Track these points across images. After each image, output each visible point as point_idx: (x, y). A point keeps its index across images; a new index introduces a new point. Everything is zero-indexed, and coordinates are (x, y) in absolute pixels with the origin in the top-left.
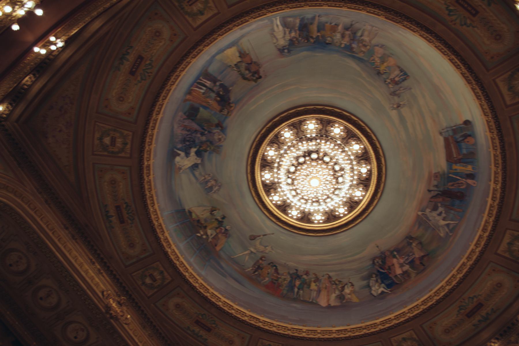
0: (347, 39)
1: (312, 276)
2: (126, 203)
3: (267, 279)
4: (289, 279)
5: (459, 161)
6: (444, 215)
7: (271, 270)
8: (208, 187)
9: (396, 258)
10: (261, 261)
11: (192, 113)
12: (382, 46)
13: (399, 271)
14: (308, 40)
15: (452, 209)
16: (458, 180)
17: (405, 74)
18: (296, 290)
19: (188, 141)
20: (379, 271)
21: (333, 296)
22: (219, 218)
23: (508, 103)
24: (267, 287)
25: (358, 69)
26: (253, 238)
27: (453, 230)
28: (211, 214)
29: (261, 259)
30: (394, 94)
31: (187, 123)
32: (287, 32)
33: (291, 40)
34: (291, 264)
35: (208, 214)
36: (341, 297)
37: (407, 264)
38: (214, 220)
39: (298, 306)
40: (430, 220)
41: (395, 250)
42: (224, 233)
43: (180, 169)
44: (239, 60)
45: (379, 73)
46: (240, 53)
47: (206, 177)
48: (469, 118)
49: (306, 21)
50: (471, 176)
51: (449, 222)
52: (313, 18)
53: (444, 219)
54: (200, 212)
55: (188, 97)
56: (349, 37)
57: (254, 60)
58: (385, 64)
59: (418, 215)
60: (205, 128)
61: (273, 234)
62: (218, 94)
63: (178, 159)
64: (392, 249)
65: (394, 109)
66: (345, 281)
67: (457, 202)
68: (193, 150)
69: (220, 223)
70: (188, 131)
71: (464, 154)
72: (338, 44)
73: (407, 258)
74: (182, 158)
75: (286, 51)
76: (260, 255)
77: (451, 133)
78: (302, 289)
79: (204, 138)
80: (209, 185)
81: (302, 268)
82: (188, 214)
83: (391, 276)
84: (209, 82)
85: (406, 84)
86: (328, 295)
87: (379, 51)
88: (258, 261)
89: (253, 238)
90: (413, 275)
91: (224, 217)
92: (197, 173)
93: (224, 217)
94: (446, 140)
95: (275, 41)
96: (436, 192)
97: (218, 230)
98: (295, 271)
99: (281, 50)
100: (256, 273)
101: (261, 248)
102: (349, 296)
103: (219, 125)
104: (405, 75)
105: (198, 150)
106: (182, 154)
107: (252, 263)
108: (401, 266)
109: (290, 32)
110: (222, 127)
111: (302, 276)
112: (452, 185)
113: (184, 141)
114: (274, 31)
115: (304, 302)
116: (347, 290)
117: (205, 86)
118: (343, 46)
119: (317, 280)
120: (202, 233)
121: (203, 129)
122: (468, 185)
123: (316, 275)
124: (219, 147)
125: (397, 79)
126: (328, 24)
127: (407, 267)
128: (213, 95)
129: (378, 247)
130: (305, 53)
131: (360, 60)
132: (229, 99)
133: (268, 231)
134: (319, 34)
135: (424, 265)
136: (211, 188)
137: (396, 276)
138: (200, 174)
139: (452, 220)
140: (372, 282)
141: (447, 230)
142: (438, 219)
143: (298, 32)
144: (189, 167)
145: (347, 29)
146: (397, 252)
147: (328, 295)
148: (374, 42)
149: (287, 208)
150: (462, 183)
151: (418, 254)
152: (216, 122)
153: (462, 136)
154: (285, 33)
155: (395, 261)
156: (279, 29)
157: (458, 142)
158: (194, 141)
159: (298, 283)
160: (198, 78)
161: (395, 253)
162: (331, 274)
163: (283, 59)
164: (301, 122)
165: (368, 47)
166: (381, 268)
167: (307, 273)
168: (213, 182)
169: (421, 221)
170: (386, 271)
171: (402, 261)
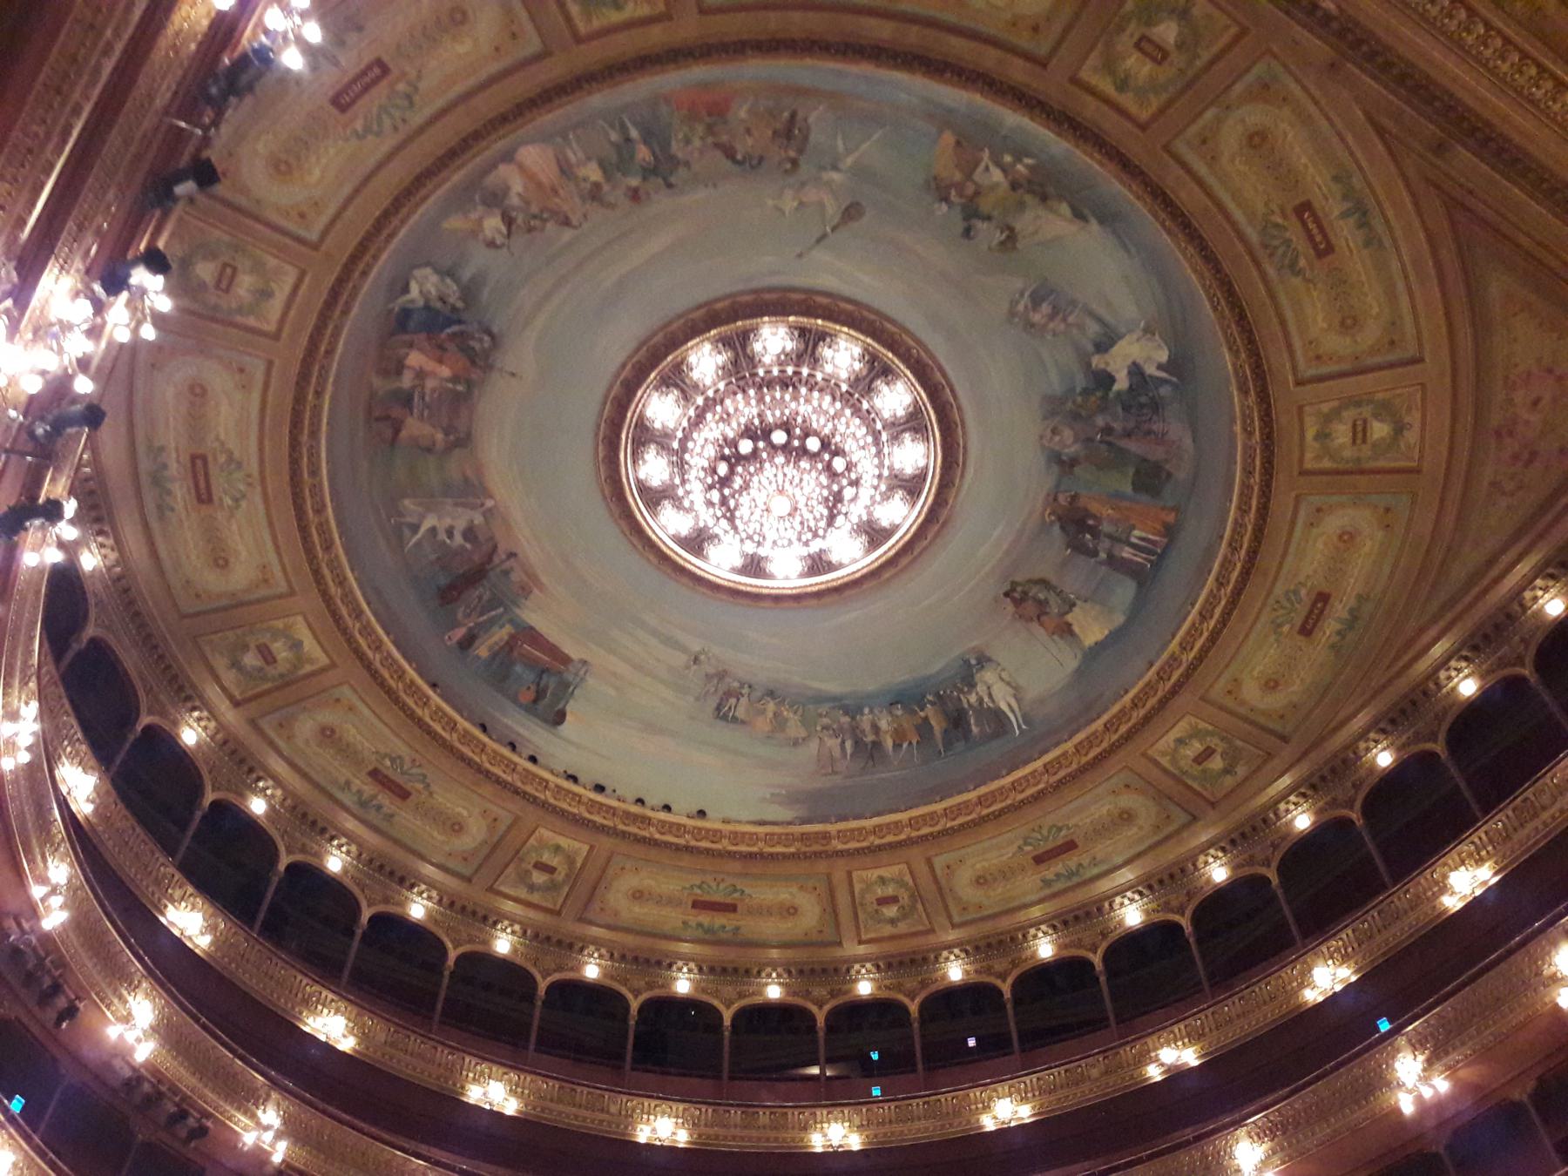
0: (866, 726)
1: (616, 195)
3: (743, 114)
4: (676, 148)
5: (510, 644)
6: (442, 536)
8: (1048, 298)
9: (448, 380)
10: (792, 154)
13: (415, 359)
14: (937, 695)
15: (438, 559)
16: (482, 614)
17: (724, 718)
18: (634, 133)
19: (1142, 406)
20: (460, 322)
21: (517, 185)
22: (981, 226)
25: (816, 685)
26: (851, 212)
28: (1011, 229)
29: (795, 163)
30: (722, 675)
31: (1158, 454)
32: (986, 699)
33: (972, 686)
34: (701, 194)
35: (1018, 226)
36: (495, 199)
37: (413, 388)
38: (995, 213)
40: (456, 505)
42: (948, 187)
43: (1148, 331)
44: (1069, 618)
45: (771, 694)
47: (1062, 326)
48: (561, 728)
50: (468, 642)
51: (419, 536)
53: (433, 530)
54: (1050, 225)
55: (1171, 518)
56: (863, 731)
57: (1035, 626)
58: (770, 715)
59: (491, 497)
60: (1103, 447)
61: (800, 256)
63: (1163, 356)
64: (476, 392)
66: (519, 240)
67: (443, 581)
69: (971, 213)
70: (1149, 432)
73: (427, 398)
74: (1149, 359)
75: (973, 662)
76: (805, 169)
78: (617, 146)
81: (662, 202)
82: (1086, 212)
83: (423, 336)
84: (1125, 555)
85: (713, 703)
87: (795, 729)
88: (801, 151)
89: (851, 212)
90: (377, 382)
91: (967, 233)
92: (1093, 328)
93: (967, 233)
94: (566, 660)
95: (1004, 675)
96: (496, 560)
97: (970, 189)
98: (673, 180)
99: (983, 660)
100: (786, 114)
101: (811, 194)
102: (474, 216)
104: (722, 714)
105: (1109, 388)
106: (1151, 370)
107: (816, 137)
108: (421, 374)
109: (981, 700)
110: (1061, 462)
111: (645, 179)
112: (480, 598)
113: (1156, 406)
114: (1015, 696)
116: (493, 224)
117: (1134, 546)
118: (866, 710)
120: (1019, 167)
121: (1109, 444)
122: (455, 624)
124: (1052, 414)
125: (733, 701)
127: (407, 381)
128: (1106, 527)
129: (513, 375)
131: (820, 698)
132: (1062, 528)
133: (820, 255)
135: (377, 419)
136: (1036, 301)
137: (411, 345)
138: (1081, 327)
139: (418, 544)
140: (452, 290)
141: (409, 519)
142: (445, 522)
144: (1121, 337)
145: (874, 743)
146: (457, 394)
148: (814, 745)
150: (469, 615)
151: (415, 427)
153: (547, 687)
154: (990, 696)
155: (445, 372)
156: (1004, 700)
157: (543, 672)
158: (1126, 409)
159: (643, 153)
161: (460, 388)
162: (568, 234)
163: (973, 644)
166: (462, 333)
167: (635, 195)
168: (1036, 318)
169: (471, 490)
170: (443, 335)
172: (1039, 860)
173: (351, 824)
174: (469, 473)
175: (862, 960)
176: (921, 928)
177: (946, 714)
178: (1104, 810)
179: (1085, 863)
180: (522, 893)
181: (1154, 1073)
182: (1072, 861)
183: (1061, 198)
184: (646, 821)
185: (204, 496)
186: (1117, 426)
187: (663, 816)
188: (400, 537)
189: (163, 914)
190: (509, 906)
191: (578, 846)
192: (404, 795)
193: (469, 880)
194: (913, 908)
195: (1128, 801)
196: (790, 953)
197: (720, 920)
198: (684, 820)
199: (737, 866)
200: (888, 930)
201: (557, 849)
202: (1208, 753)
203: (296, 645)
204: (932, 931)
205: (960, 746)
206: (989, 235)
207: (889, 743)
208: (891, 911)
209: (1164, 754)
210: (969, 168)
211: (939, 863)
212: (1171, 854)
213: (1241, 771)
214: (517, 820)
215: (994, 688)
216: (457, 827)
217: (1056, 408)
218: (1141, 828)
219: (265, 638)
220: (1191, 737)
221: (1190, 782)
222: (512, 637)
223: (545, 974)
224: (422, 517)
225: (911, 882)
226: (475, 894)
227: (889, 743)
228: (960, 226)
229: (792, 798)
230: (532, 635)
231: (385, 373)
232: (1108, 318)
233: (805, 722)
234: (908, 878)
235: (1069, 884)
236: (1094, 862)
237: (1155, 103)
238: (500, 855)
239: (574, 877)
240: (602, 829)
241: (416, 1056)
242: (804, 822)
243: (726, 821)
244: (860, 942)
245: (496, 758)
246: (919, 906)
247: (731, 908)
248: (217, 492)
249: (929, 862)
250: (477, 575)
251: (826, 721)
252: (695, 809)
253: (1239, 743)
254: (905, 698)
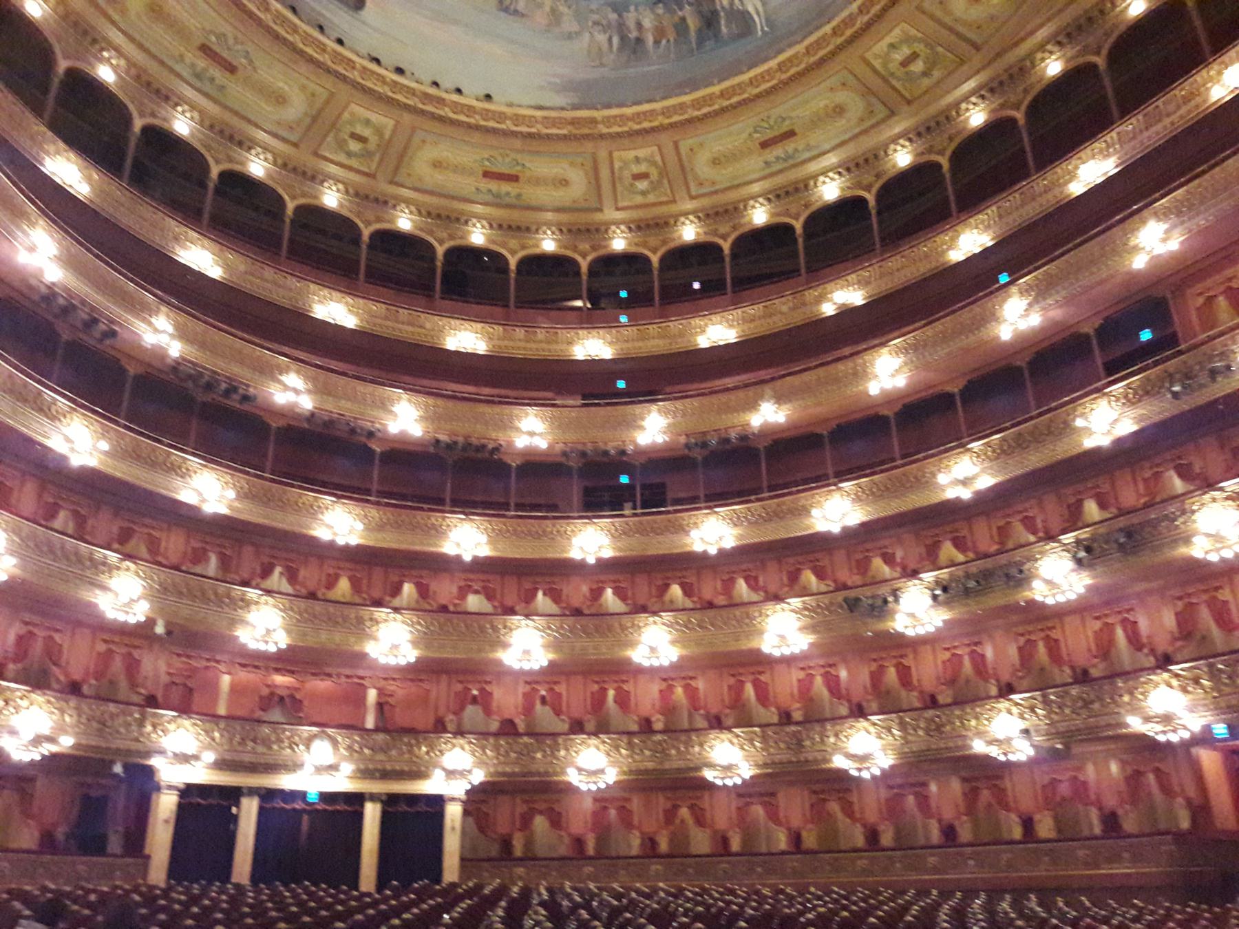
0: (631, 23)
12: (569, 36)
17: (506, 10)
23: (353, 105)
58: (547, 9)
72: (641, 9)
87: (569, 24)
118: (632, 8)
126: (672, 39)
134: (680, 13)
143: (719, 8)
148: (587, 36)
165: (590, 24)
172: (765, 145)
173: (189, 93)
175: (617, 223)
176: (664, 199)
178: (822, 104)
179: (800, 148)
180: (342, 158)
181: (828, 309)
182: (790, 146)
184: (441, 101)
187: (455, 97)
189: (43, 165)
190: (333, 169)
191: (383, 120)
192: (231, 69)
193: (295, 145)
194: (660, 182)
195: (842, 97)
196: (564, 218)
197: (505, 187)
198: (475, 103)
199: (518, 143)
200: (639, 199)
201: (367, 122)
202: (914, 56)
204: (674, 201)
205: (709, 44)
207: (650, 40)
208: (642, 185)
209: (876, 56)
211: (684, 146)
212: (868, 142)
213: (937, 74)
214: (332, 94)
216: (280, 100)
218: (848, 121)
220: (901, 42)
221: (894, 82)
223: (368, 223)
225: (660, 163)
226: (303, 157)
227: (650, 40)
229: (568, 86)
234: (658, 158)
235: (786, 165)
236: (808, 148)
238: (320, 125)
239: (385, 147)
240: (407, 107)
241: (274, 283)
242: (575, 107)
243: (510, 105)
244: (618, 209)
245: (307, 38)
246: (665, 181)
247: (513, 178)
249: (676, 145)
251: (596, 17)
252: (482, 93)
253: (940, 49)
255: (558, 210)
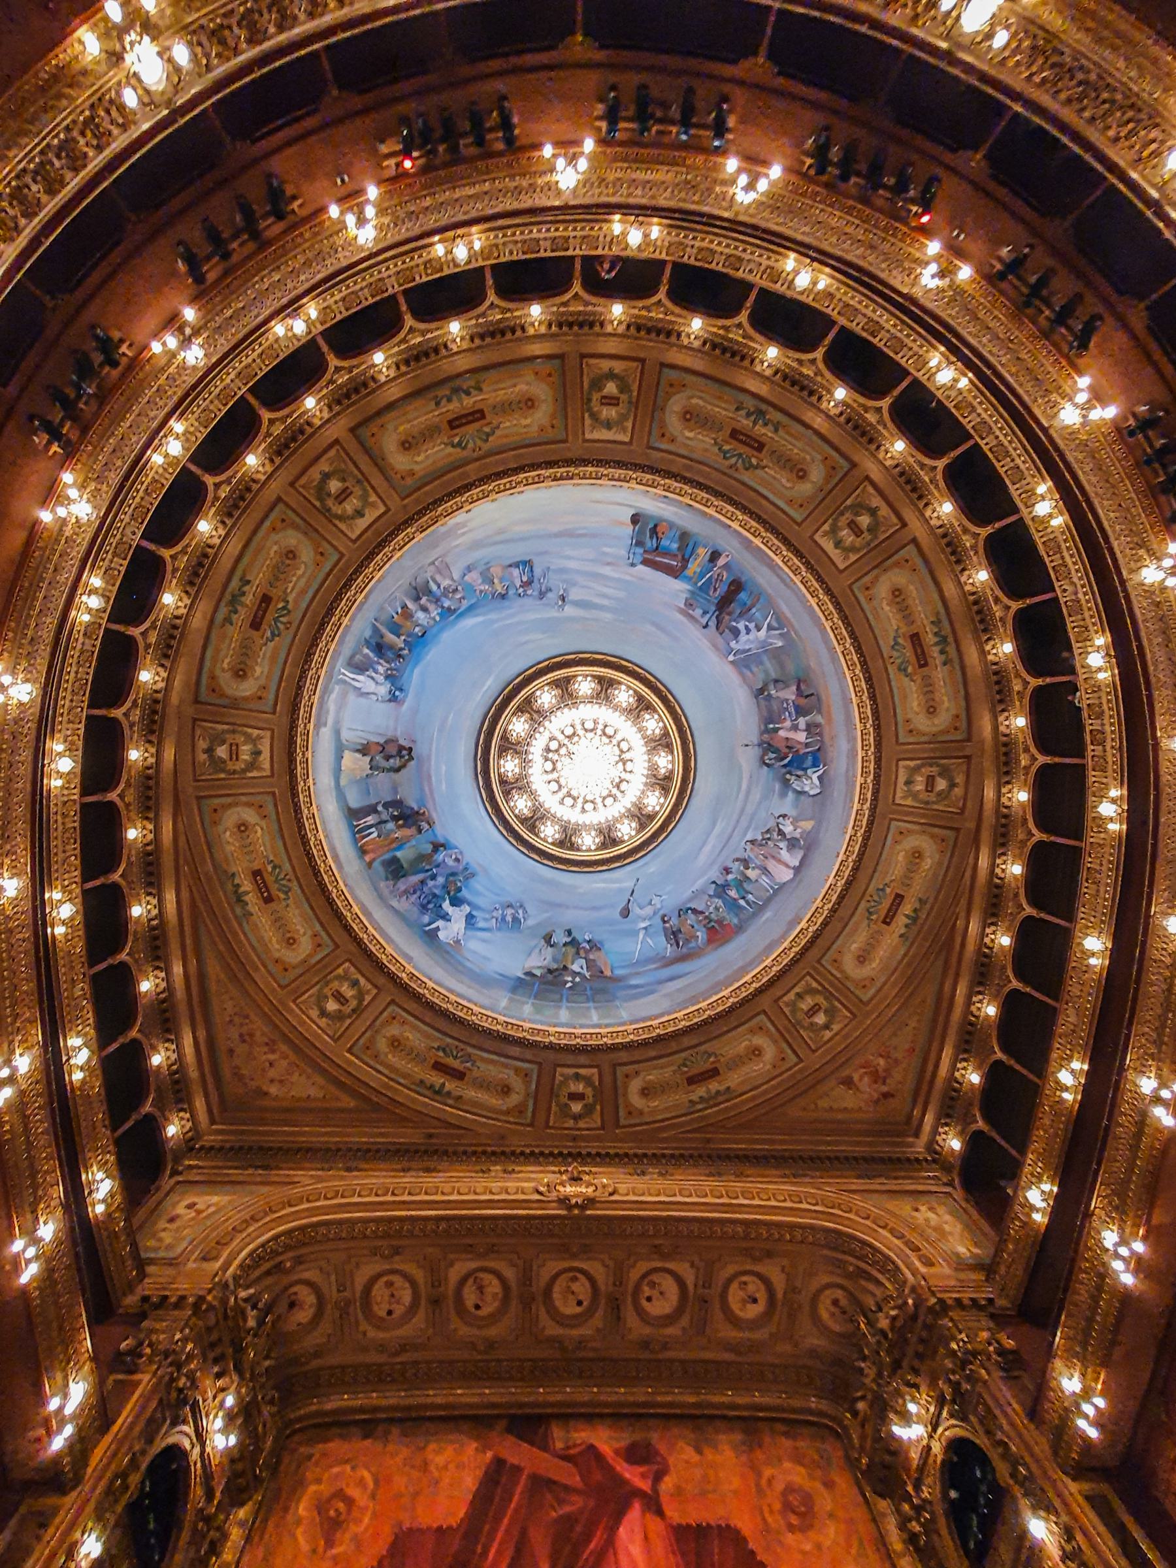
0: (431, 607)
1: (736, 867)
2: (438, 1049)
4: (720, 903)
5: (685, 561)
6: (752, 626)
7: (691, 919)
8: (511, 920)
11: (395, 870)
12: (469, 569)
13: (801, 737)
14: (400, 656)
17: (525, 563)
18: (742, 902)
20: (785, 766)
21: (785, 854)
24: (710, 941)
25: (480, 619)
26: (625, 913)
27: (781, 622)
30: (542, 595)
31: (402, 885)
33: (387, 677)
36: (793, 844)
39: (768, 914)
41: (767, 723)
44: (368, 759)
45: (503, 597)
46: (358, 751)
48: (632, 512)
49: (373, 642)
50: (715, 556)
52: (375, 630)
54: (540, 960)
55: (367, 858)
57: (382, 741)
62: (395, 818)
63: (441, 935)
65: (562, 607)
67: (743, 596)
68: (446, 905)
69: (574, 943)
71: (679, 549)
76: (657, 920)
77: (640, 550)
79: (441, 880)
80: (509, 918)
81: (714, 874)
85: (538, 571)
86: (780, 861)
87: (474, 577)
88: (665, 929)
90: (819, 719)
91: (569, 932)
93: (569, 932)
94: (645, 562)
97: (582, 953)
99: (393, 699)
101: (649, 910)
103: (437, 847)
108: (795, 728)
110: (443, 845)
113: (424, 908)
115: (768, 900)
116: (788, 829)
119: (746, 863)
122: (726, 566)
123: (737, 860)
125: (525, 579)
127: (802, 722)
128: (391, 825)
130: (417, 671)
133: (629, 884)
136: (515, 919)
137: (807, 745)
138: (486, 920)
140: (796, 785)
145: (417, 599)
147: (780, 861)
148: (456, 576)
149: (613, 835)
151: (790, 694)
152: (429, 848)
155: (782, 733)
156: (363, 681)
158: (435, 895)
159: (733, 893)
160: (352, 827)
162: (749, 837)
164: (505, 737)
168: (510, 911)
169: (744, 662)
171: (788, 724)
174: (748, 673)
177: (391, 647)
178: (258, 670)
183: (542, 976)
185: (915, 639)
186: (431, 883)
188: (778, 619)
197: (454, 407)
203: (838, 544)
205: (368, 633)
206: (560, 938)
207: (410, 605)
210: (590, 964)
215: (374, 684)
217: (469, 874)
218: (223, 670)
219: (858, 542)
221: (226, 727)
222: (685, 567)
224: (768, 637)
225: (337, 522)
226: (651, 348)
228: (574, 934)
230: (674, 573)
231: (818, 725)
232: (480, 934)
233: (470, 588)
236: (228, 620)
237: (559, 1078)
248: (908, 644)
250: (724, 604)
254: (419, 641)
255: (390, 406)
